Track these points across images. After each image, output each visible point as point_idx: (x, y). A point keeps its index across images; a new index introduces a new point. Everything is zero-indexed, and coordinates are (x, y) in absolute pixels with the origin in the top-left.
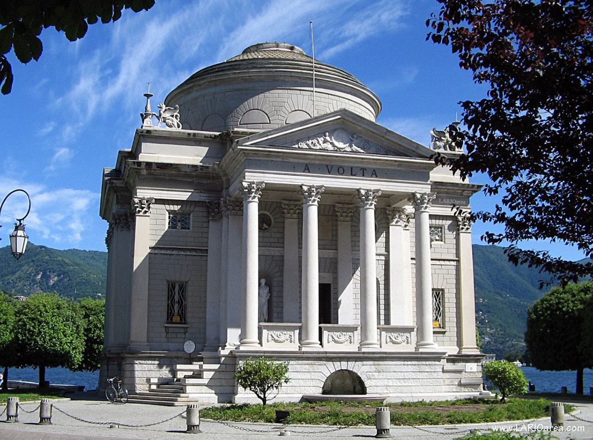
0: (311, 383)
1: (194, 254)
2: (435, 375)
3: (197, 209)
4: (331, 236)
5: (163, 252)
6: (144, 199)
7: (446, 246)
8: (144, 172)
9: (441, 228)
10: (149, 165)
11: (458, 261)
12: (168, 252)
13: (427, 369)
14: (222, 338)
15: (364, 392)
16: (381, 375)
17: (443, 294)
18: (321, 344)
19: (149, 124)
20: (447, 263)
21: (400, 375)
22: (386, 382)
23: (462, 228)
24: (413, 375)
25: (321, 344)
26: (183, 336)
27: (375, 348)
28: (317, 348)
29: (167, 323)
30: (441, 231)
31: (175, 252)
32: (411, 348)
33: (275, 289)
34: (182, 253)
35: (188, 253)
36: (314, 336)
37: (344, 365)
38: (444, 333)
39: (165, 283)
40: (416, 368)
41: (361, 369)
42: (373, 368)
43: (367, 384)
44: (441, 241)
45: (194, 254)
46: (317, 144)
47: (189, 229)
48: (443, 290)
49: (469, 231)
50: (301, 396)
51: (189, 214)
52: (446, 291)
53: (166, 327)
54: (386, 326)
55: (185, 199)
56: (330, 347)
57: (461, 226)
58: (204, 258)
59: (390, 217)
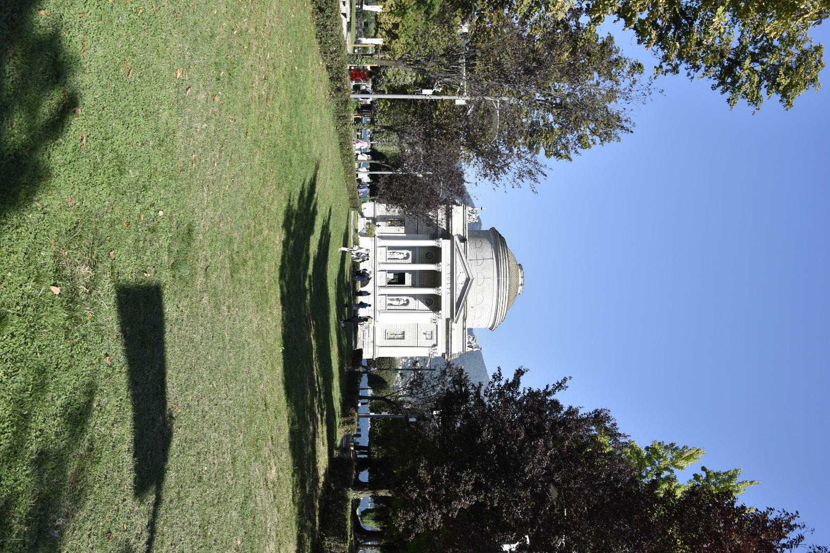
56: (378, 274)
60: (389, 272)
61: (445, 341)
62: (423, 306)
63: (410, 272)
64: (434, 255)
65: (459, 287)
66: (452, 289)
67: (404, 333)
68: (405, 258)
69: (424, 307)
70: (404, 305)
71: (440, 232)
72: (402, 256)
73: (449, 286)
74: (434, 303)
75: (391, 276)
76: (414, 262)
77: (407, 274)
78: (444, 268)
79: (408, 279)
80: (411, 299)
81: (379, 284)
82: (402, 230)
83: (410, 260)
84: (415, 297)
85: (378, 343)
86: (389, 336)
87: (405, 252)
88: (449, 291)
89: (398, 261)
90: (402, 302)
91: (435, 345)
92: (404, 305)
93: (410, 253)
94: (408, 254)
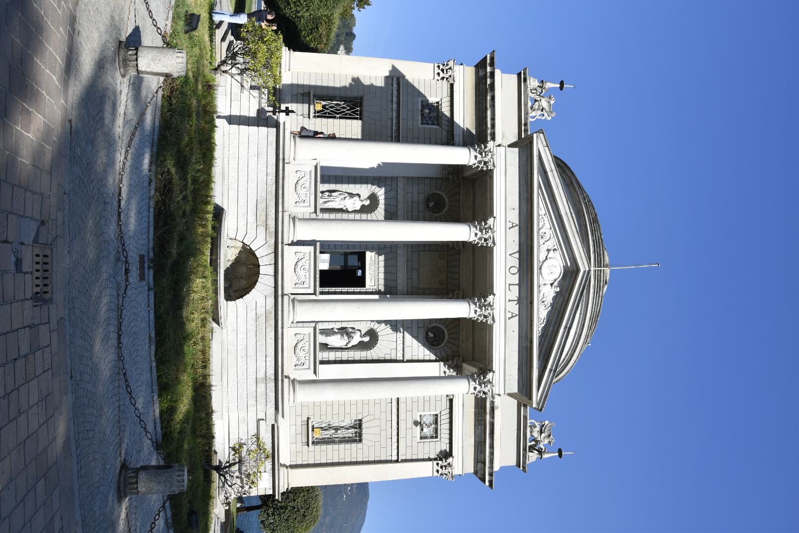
0: (242, 223)
1: (394, 128)
2: (252, 401)
3: (445, 133)
4: (422, 286)
5: (395, 92)
6: (453, 72)
7: (415, 444)
8: (481, 73)
9: (436, 437)
10: (492, 75)
11: (397, 461)
12: (395, 99)
13: (261, 387)
14: (301, 91)
15: (229, 297)
16: (252, 323)
17: (355, 441)
18: (293, 244)
19: (533, 83)
20: (395, 446)
21: (251, 350)
22: (242, 329)
23: (438, 464)
24: (252, 369)
25: (293, 244)
26: (300, 113)
27: (289, 316)
28: (289, 237)
29: (314, 96)
30: (432, 437)
31: (395, 106)
32: (289, 369)
33: (358, 216)
34: (395, 115)
35: (394, 122)
36: (305, 232)
37: (266, 270)
38: (308, 445)
39: (361, 94)
40: (261, 374)
41: (260, 295)
42: (261, 311)
43: (239, 301)
44: (421, 438)
45: (394, 128)
46: (544, 239)
47: (422, 124)
48: (360, 441)
49: (436, 474)
50: (225, 207)
51: (438, 125)
52: (360, 445)
53: (309, 93)
54: (318, 332)
55: (455, 120)
56: (290, 254)
57: (440, 462)
58: (390, 138)
59: (451, 362)
60: (326, 247)
61: (471, 441)
62: (416, 348)
63: (380, 247)
64: (460, 196)
65: (545, 293)
66: (526, 300)
67: (359, 425)
68: (364, 210)
69: (423, 352)
70: (362, 346)
71: (458, 138)
72: (354, 204)
73: (515, 292)
74: (460, 348)
75: (324, 263)
76: (391, 215)
77: (370, 256)
78: (502, 233)
79: (375, 270)
80: (384, 332)
81: (289, 288)
82: (354, 127)
83: (380, 211)
84: (395, 325)
85: (285, 457)
86: (318, 434)
87: (365, 190)
88: (514, 308)
89: (345, 216)
90: (356, 339)
91: (446, 455)
92: (362, 346)
93: (381, 193)
94: (373, 198)
